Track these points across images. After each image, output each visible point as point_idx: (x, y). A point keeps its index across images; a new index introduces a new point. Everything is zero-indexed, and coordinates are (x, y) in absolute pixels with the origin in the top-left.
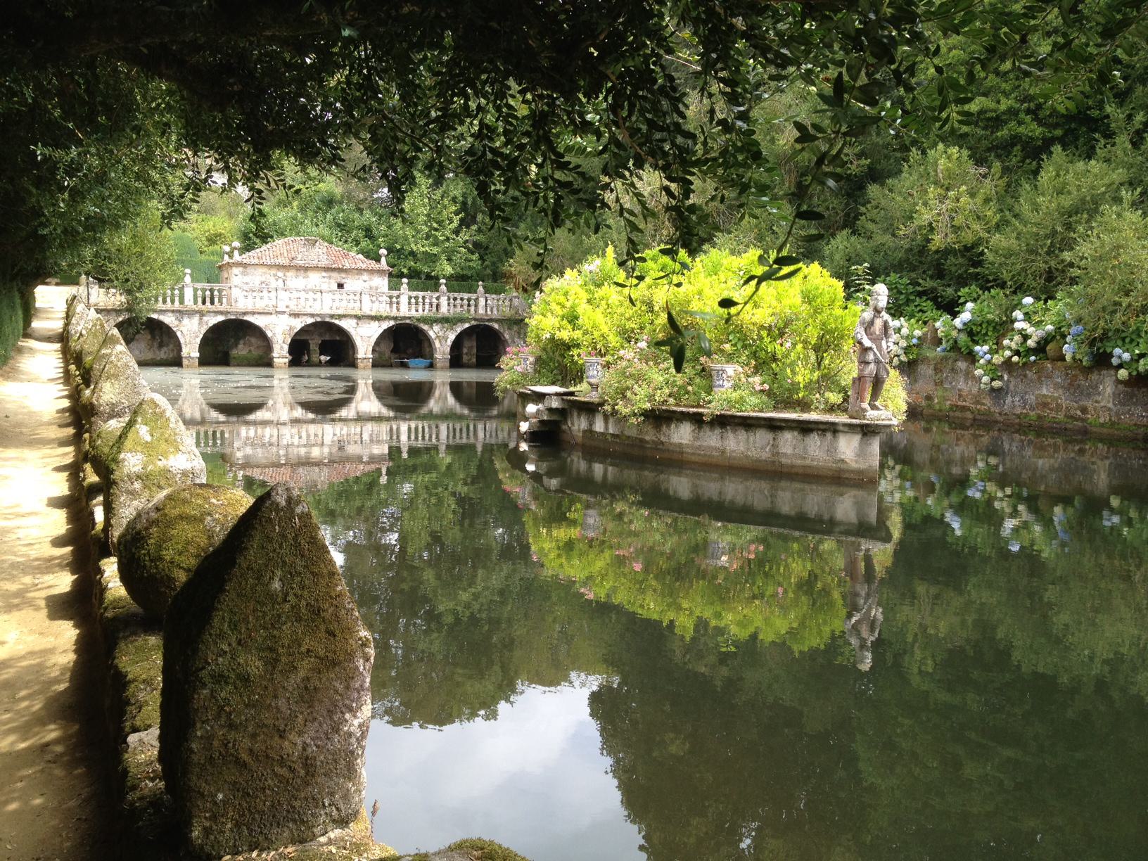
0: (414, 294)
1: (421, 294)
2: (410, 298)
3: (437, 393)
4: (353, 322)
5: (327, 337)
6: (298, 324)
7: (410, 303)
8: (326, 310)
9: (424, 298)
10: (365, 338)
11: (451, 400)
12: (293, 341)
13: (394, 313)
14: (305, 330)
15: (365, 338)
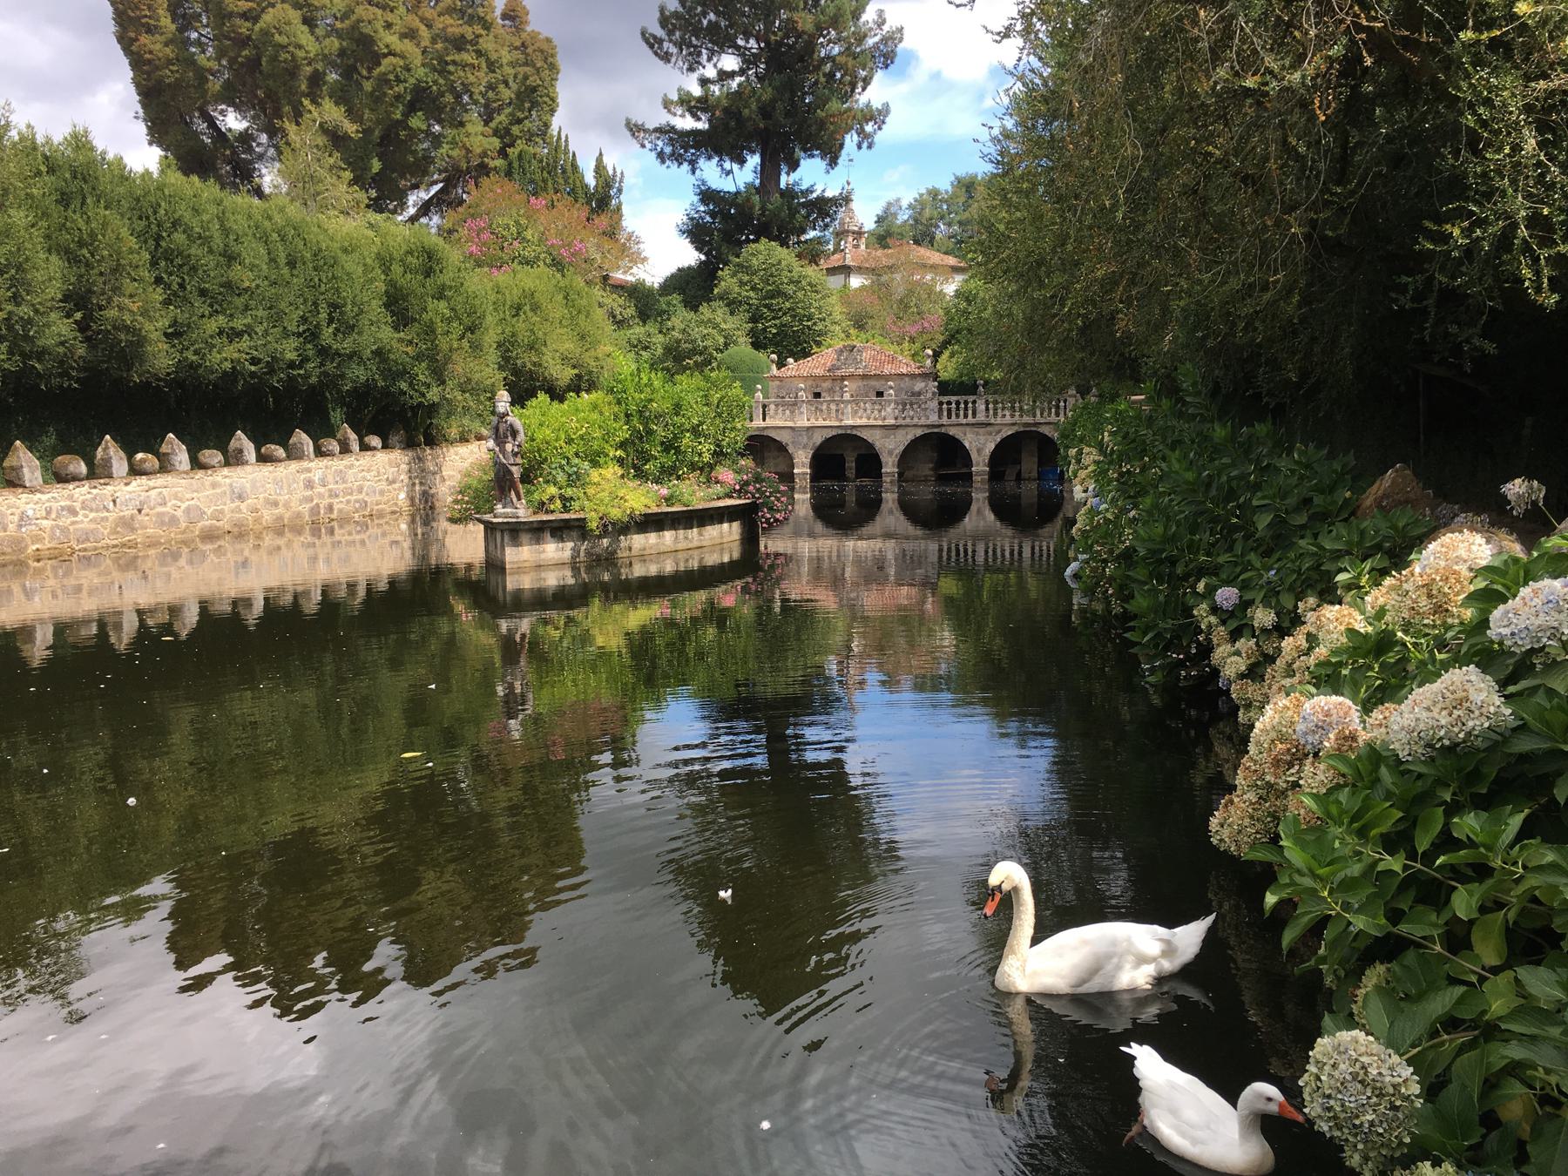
0: (945, 399)
1: (953, 399)
2: (941, 403)
3: (974, 507)
4: (878, 432)
5: (863, 451)
6: (818, 439)
7: (940, 410)
8: (850, 422)
9: (958, 403)
10: (890, 448)
11: (991, 517)
12: (814, 457)
13: (923, 421)
14: (828, 441)
15: (890, 448)
